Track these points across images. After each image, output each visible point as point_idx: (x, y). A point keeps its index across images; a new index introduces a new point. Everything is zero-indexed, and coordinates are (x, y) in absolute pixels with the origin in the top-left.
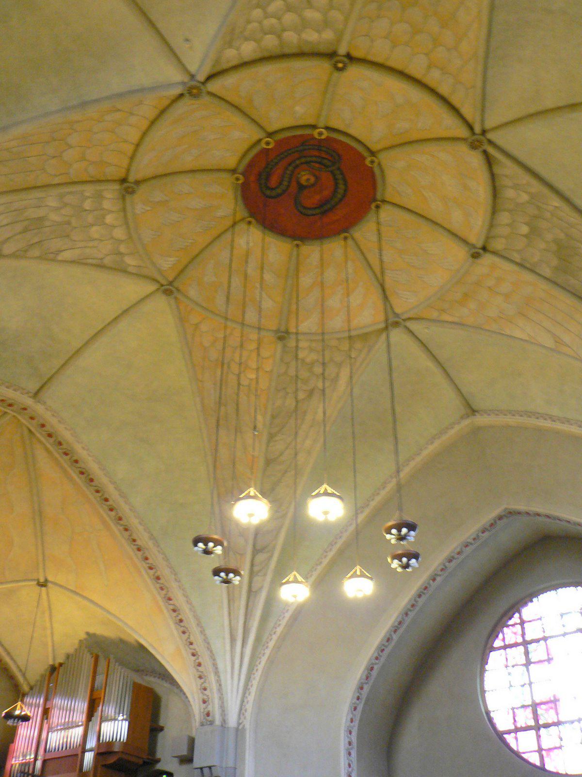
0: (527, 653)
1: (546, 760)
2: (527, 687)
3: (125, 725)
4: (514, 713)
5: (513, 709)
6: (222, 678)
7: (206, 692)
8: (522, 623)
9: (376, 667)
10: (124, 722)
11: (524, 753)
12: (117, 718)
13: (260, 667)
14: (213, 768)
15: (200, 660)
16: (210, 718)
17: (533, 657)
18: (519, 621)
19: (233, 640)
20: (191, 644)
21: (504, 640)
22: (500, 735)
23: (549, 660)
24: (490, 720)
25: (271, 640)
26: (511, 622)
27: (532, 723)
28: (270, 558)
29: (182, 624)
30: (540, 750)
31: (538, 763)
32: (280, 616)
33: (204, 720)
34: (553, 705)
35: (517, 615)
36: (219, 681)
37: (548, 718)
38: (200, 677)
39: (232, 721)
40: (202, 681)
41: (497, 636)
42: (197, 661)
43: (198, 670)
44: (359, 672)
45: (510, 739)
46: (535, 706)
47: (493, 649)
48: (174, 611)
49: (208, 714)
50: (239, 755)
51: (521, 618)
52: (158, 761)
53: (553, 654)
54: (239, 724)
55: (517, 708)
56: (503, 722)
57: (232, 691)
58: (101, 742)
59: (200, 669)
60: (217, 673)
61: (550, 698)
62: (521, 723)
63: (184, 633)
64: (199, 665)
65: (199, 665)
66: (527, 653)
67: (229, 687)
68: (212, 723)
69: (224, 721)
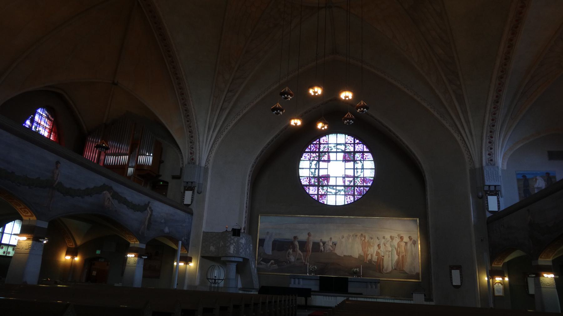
3: (151, 158)
4: (310, 179)
5: (310, 177)
6: (201, 143)
7: (193, 150)
8: (320, 144)
10: (151, 157)
12: (145, 154)
14: (193, 183)
15: (193, 135)
16: (193, 161)
20: (190, 127)
21: (310, 149)
25: (224, 131)
26: (315, 142)
30: (318, 194)
31: (316, 199)
32: (230, 121)
33: (190, 162)
34: (326, 179)
35: (318, 140)
38: (191, 142)
39: (203, 164)
40: (192, 144)
41: (308, 147)
43: (190, 139)
44: (259, 152)
46: (319, 177)
48: (186, 110)
50: (205, 180)
52: (160, 176)
54: (206, 166)
57: (205, 151)
58: (138, 164)
59: (192, 139)
61: (326, 176)
63: (188, 121)
64: (192, 137)
65: (192, 137)
66: (319, 156)
68: (194, 163)
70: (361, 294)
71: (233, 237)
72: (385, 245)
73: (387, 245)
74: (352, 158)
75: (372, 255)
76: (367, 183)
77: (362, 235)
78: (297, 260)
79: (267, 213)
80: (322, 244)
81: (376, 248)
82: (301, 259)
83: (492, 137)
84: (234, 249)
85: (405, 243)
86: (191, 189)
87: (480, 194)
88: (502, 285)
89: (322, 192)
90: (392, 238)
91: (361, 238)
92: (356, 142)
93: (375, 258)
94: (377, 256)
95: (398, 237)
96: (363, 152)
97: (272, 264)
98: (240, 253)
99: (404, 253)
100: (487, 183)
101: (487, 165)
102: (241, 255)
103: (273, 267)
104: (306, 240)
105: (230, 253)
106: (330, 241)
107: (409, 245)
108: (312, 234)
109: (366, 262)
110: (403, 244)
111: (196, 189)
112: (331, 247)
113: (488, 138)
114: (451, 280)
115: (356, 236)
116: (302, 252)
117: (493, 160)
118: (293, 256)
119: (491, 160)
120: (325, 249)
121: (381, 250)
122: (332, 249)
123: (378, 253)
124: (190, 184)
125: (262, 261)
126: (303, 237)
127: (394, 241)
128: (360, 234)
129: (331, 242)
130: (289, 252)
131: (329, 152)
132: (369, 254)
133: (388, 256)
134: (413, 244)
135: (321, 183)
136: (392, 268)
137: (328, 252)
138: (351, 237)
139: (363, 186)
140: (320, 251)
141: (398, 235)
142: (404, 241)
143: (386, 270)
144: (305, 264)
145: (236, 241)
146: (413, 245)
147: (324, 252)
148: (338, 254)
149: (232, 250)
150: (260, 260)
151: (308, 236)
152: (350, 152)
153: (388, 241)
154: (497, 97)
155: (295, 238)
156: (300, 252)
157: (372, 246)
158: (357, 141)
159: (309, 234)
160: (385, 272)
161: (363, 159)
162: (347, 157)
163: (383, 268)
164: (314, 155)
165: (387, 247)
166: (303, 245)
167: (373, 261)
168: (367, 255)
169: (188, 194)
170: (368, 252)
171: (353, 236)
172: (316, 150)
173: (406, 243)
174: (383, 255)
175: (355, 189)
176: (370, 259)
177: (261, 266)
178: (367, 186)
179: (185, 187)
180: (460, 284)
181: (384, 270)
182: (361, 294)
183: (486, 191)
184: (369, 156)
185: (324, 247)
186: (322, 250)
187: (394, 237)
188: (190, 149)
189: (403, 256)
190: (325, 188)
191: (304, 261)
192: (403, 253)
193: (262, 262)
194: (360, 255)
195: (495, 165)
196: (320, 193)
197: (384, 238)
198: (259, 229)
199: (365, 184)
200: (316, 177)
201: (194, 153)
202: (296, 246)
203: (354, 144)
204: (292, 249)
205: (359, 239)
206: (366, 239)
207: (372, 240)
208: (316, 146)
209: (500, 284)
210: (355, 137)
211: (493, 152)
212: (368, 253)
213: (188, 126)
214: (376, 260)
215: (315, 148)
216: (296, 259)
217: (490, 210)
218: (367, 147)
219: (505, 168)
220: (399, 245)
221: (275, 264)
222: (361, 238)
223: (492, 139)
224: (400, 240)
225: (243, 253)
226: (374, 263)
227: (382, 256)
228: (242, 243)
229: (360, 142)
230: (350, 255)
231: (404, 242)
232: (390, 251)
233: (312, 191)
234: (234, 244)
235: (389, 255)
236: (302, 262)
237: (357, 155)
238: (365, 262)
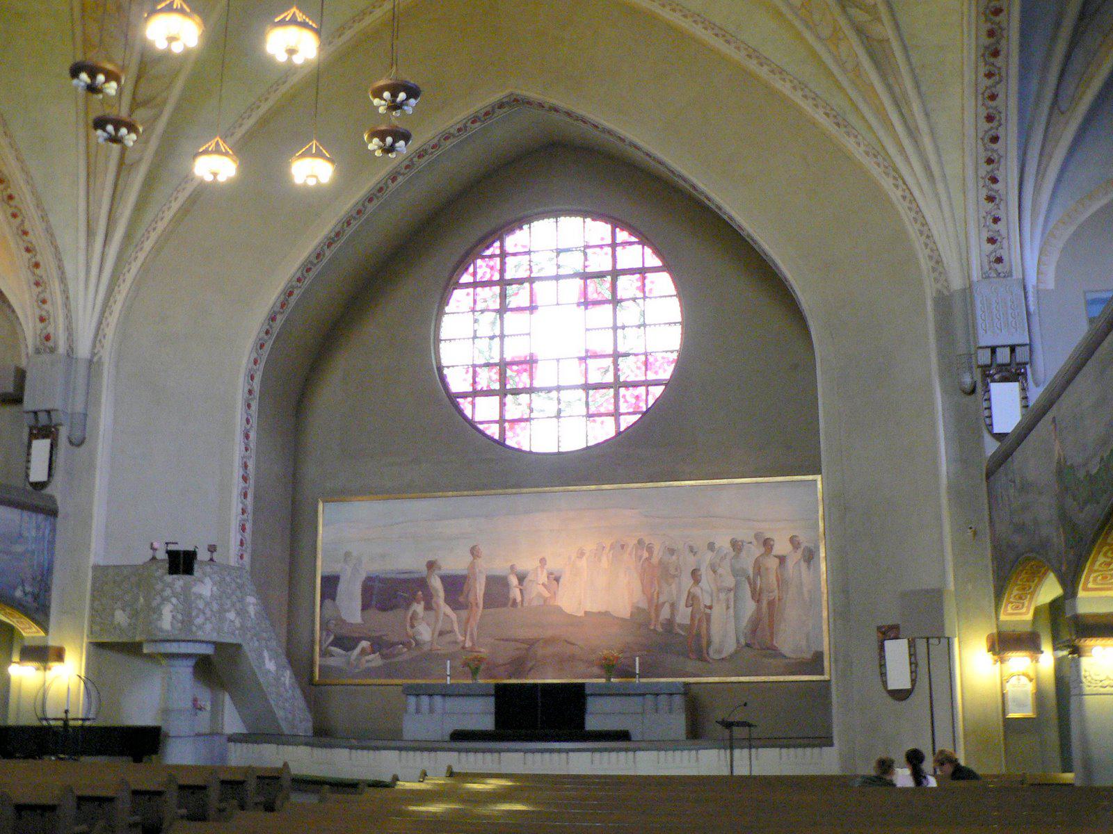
0: (503, 296)
1: (509, 434)
2: (497, 340)
4: (475, 372)
5: (474, 366)
6: (71, 287)
7: (45, 306)
8: (503, 255)
9: (296, 292)
11: (481, 423)
13: (130, 277)
15: (39, 258)
16: (50, 344)
17: (513, 302)
18: (498, 252)
19: (90, 233)
20: (25, 233)
21: (474, 274)
22: (453, 398)
23: (532, 308)
24: (443, 378)
25: (148, 239)
26: (488, 252)
27: (496, 386)
28: (156, 118)
29: (12, 203)
30: (502, 421)
31: (497, 437)
32: (165, 205)
33: (42, 347)
34: (527, 367)
35: (497, 244)
36: (65, 292)
37: (517, 379)
38: (37, 284)
40: (40, 289)
41: (467, 269)
42: (34, 260)
43: (34, 274)
44: (272, 296)
45: (465, 405)
46: (503, 366)
47: (459, 286)
49: (47, 338)
51: (502, 247)
53: (539, 300)
54: (93, 354)
55: (480, 366)
56: (458, 382)
57: (85, 307)
59: (37, 271)
60: (63, 280)
61: (526, 357)
62: (482, 384)
64: (37, 265)
65: (37, 265)
66: (503, 296)
67: (81, 302)
68: (53, 350)
69: (71, 350)
70: (623, 736)
71: (169, 578)
72: (715, 572)
73: (720, 571)
74: (608, 295)
76: (656, 373)
77: (640, 542)
78: (441, 634)
79: (340, 495)
80: (514, 581)
81: (687, 582)
82: (452, 631)
83: (994, 180)
84: (173, 617)
85: (777, 561)
86: (46, 431)
87: (967, 380)
88: (1031, 680)
89: (513, 411)
90: (736, 546)
92: (618, 241)
93: (683, 616)
94: (691, 608)
95: (755, 542)
96: (642, 271)
97: (363, 652)
98: (194, 629)
99: (776, 592)
100: (986, 339)
101: (986, 277)
102: (201, 635)
103: (367, 661)
104: (465, 572)
105: (161, 630)
106: (539, 569)
107: (790, 563)
108: (484, 550)
110: (772, 563)
111: (63, 433)
112: (543, 588)
113: (981, 183)
114: (883, 675)
115: (623, 547)
116: (454, 609)
117: (1005, 258)
118: (428, 624)
119: (999, 260)
120: (526, 597)
121: (701, 589)
122: (546, 594)
123: (692, 599)
124: (43, 419)
125: (333, 644)
126: (455, 563)
127: (743, 554)
129: (542, 574)
130: (415, 611)
131: (531, 280)
132: (664, 603)
133: (724, 606)
134: (805, 561)
135: (511, 382)
137: (535, 603)
138: (607, 550)
139: (647, 384)
140: (510, 603)
141: (757, 536)
142: (774, 554)
143: (720, 651)
144: (463, 648)
145: (179, 590)
146: (803, 565)
147: (522, 604)
148: (568, 611)
149: (167, 620)
150: (327, 643)
151: (469, 558)
152: (601, 275)
153: (723, 558)
154: (991, 33)
155: (431, 565)
156: (448, 610)
157: (674, 577)
158: (622, 236)
159: (474, 552)
160: (717, 657)
161: (644, 292)
162: (591, 289)
163: (709, 643)
164: (483, 293)
165: (721, 576)
166: (456, 586)
167: (679, 625)
168: (658, 607)
169: (41, 448)
170: (660, 596)
171: (612, 547)
172: (492, 276)
173: (782, 559)
174: (708, 604)
177: (331, 662)
178: (656, 383)
179: (31, 429)
180: (908, 686)
181: (711, 651)
182: (623, 736)
183: (985, 368)
184: (663, 283)
185: (520, 590)
186: (515, 600)
187: (742, 542)
188: (39, 307)
189: (771, 604)
190: (524, 398)
191: (461, 638)
192: (772, 592)
193: (333, 648)
194: (638, 608)
195: (1009, 274)
196: (508, 416)
197: (711, 546)
198: (320, 543)
199: (651, 376)
200: (495, 365)
201: (51, 320)
202: (437, 591)
203: (614, 245)
204: (422, 603)
205: (633, 556)
206: (655, 553)
207: (674, 558)
208: (492, 263)
209: (1024, 680)
210: (617, 222)
211: (1004, 232)
212: (662, 600)
213: (20, 232)
214: (687, 621)
215: (488, 270)
216: (437, 633)
217: (997, 430)
218: (657, 252)
219: (1050, 284)
220: (758, 568)
221: (374, 653)
223: (995, 186)
224: (762, 550)
225: (208, 627)
227: (706, 606)
228: (200, 596)
229: (633, 239)
230: (603, 609)
231: (776, 556)
232: (730, 590)
233: (484, 411)
234: (174, 600)
235: (728, 600)
236: (456, 642)
237: (623, 281)
238: (652, 627)
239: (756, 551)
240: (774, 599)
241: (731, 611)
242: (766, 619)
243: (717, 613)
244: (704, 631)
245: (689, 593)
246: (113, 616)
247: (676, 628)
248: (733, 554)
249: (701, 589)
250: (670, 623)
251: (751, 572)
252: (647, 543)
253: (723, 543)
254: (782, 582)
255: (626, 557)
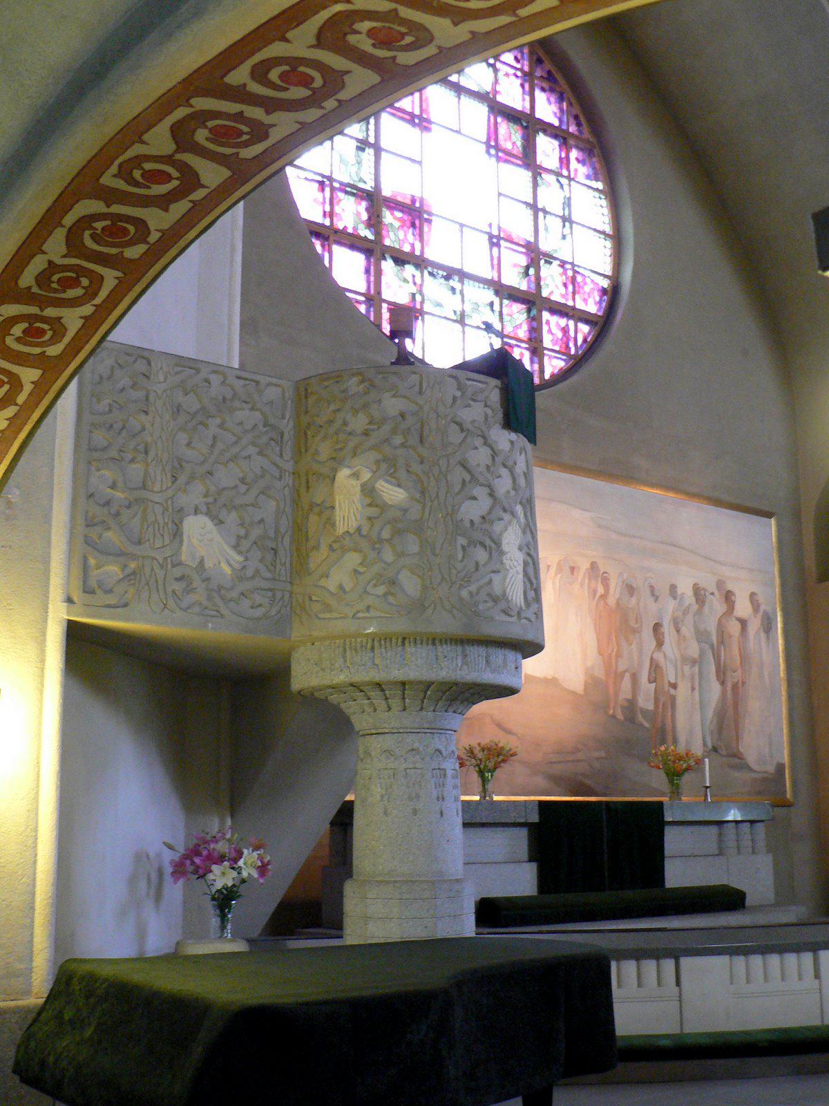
37: (397, 235)
73: (684, 630)
75: (635, 678)
90: (699, 594)
91: (593, 582)
99: (739, 673)
109: (613, 716)
110: (734, 628)
115: (573, 569)
128: (588, 566)
135: (391, 234)
136: (705, 744)
146: (763, 635)
153: (685, 612)
165: (684, 637)
170: (619, 659)
173: (743, 623)
174: (673, 681)
175: (544, 321)
176: (630, 697)
189: (735, 687)
207: (634, 600)
214: (651, 707)
222: (593, 581)
226: (644, 717)
238: (611, 712)
239: (719, 607)
240: (738, 681)
241: (697, 693)
242: (731, 711)
243: (683, 694)
244: (669, 721)
245: (652, 659)
246: (177, 534)
247: (640, 718)
248: (696, 607)
249: (665, 654)
250: (631, 707)
251: (714, 639)
252: (601, 573)
253: (685, 588)
254: (744, 657)
255: (576, 587)
